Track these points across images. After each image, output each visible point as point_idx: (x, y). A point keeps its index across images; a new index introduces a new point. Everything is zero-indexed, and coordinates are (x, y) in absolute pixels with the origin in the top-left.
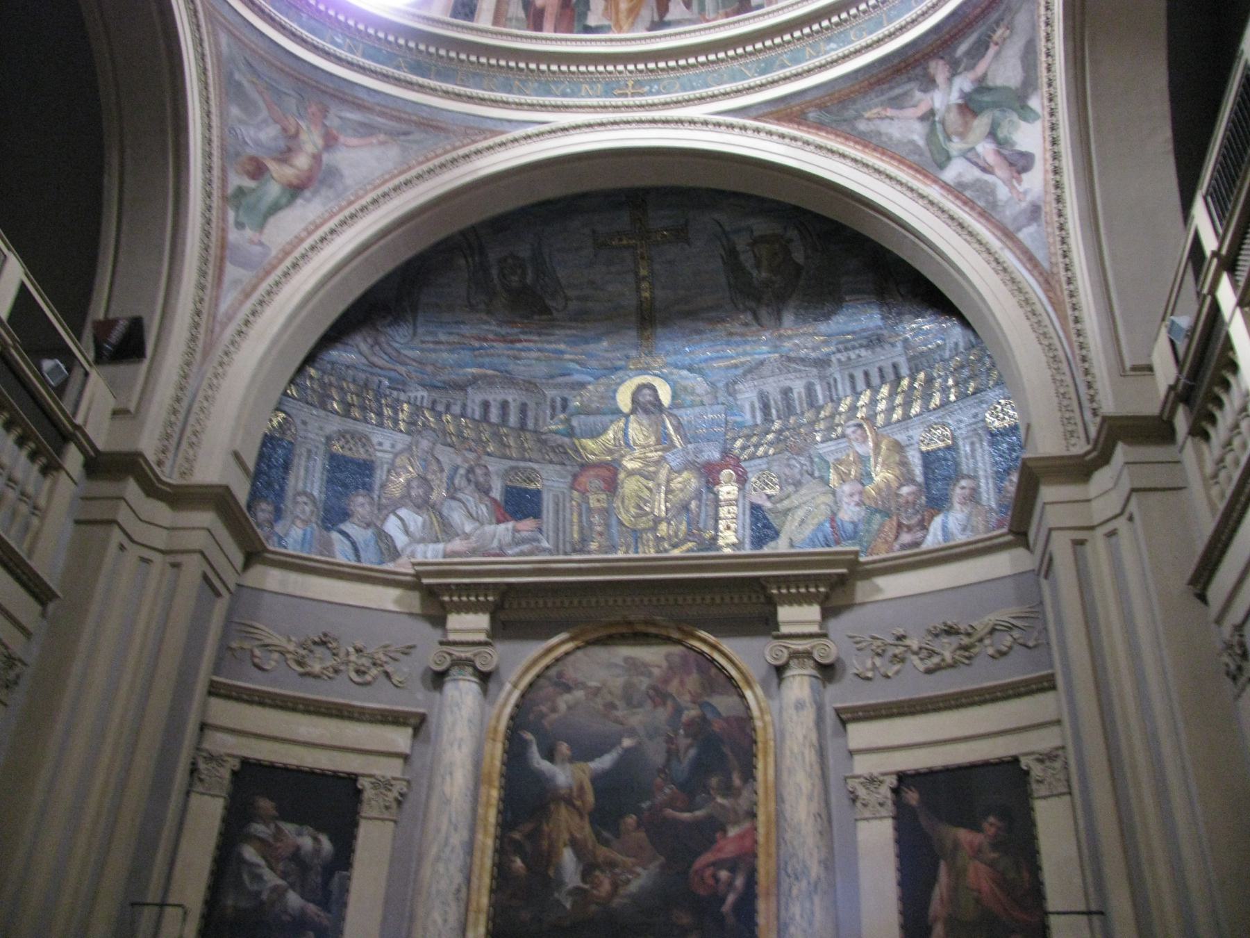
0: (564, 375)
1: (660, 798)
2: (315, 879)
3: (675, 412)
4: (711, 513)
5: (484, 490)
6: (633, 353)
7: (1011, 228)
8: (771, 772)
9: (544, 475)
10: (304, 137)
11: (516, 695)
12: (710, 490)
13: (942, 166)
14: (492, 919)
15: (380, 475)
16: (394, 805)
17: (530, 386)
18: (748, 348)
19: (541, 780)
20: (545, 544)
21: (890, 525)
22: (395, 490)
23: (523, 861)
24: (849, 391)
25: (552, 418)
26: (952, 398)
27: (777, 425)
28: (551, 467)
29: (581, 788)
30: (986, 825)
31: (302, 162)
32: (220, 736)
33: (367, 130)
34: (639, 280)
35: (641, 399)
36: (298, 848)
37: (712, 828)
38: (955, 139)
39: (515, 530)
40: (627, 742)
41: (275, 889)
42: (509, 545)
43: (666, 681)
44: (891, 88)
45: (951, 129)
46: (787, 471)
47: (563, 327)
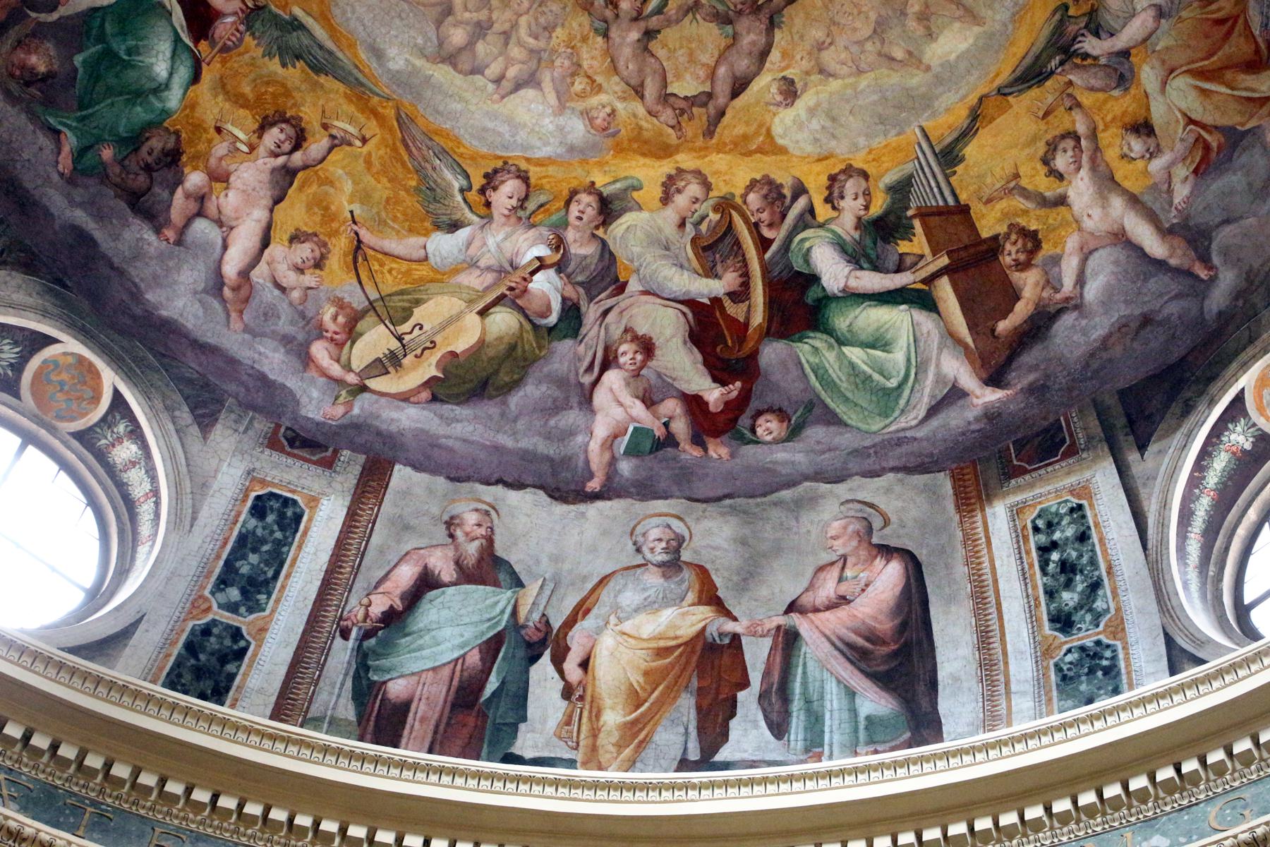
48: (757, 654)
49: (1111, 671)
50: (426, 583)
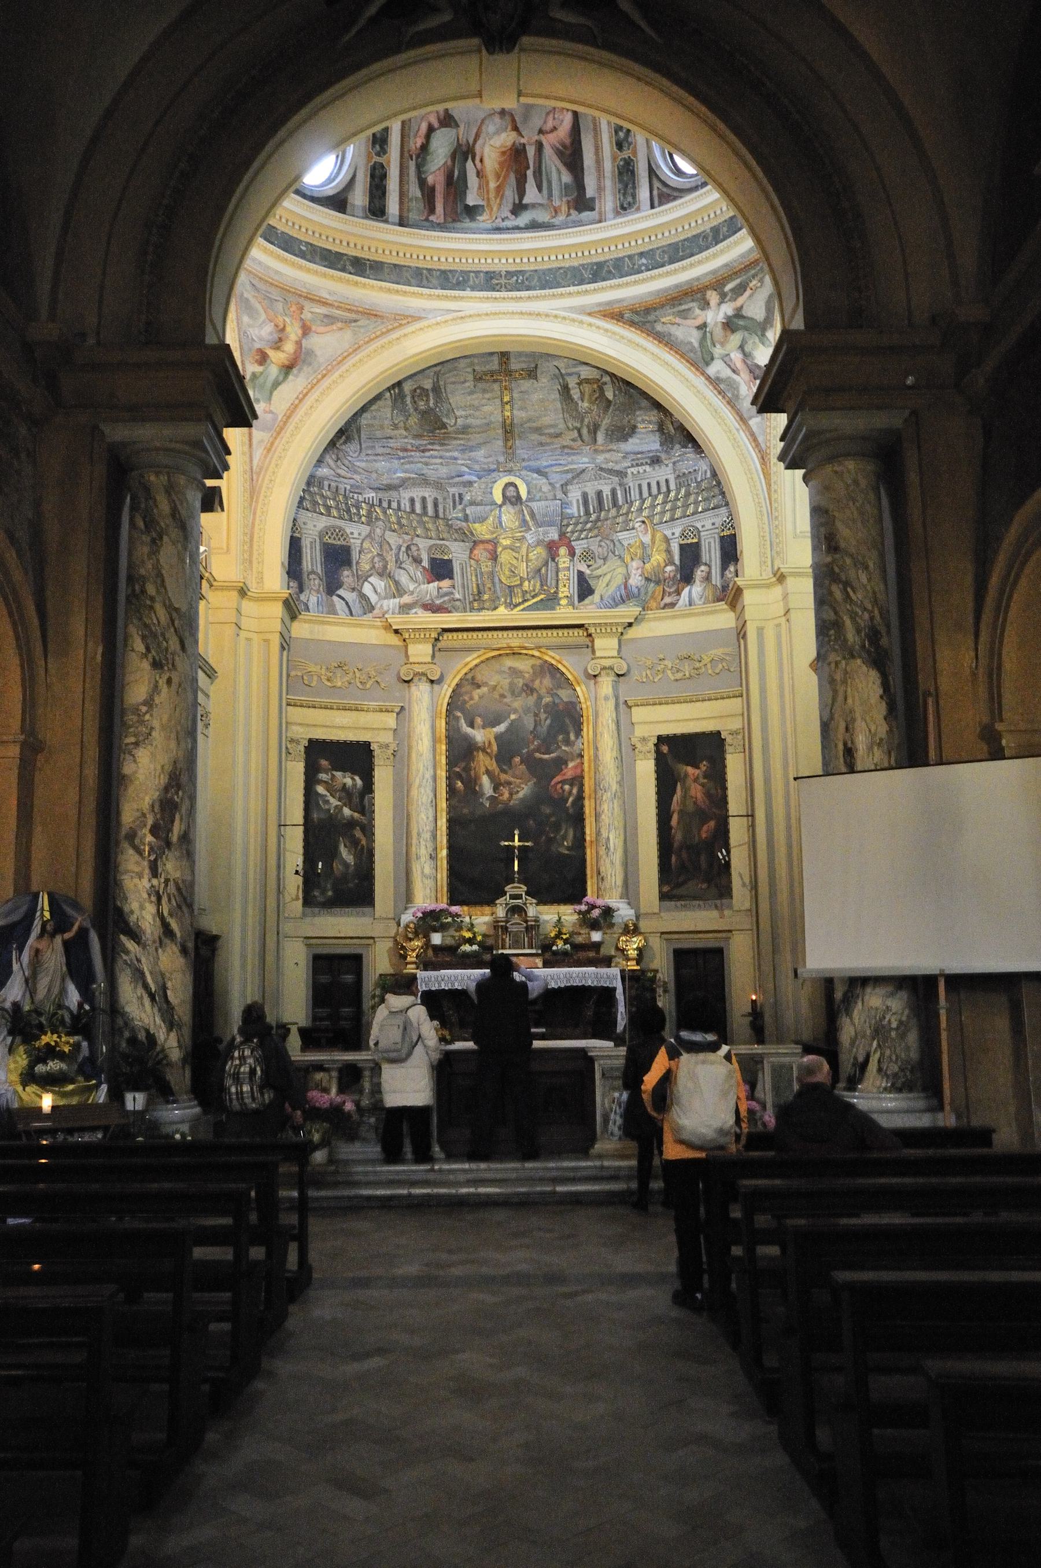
0: (459, 476)
1: (532, 747)
2: (356, 800)
3: (529, 504)
4: (554, 575)
5: (417, 561)
6: (502, 459)
7: (745, 416)
8: (591, 733)
9: (453, 550)
10: (288, 329)
11: (450, 690)
12: (553, 560)
13: (707, 364)
14: (448, 813)
15: (355, 555)
16: (392, 757)
17: (438, 485)
18: (574, 458)
19: (467, 738)
20: (457, 596)
21: (659, 589)
22: (366, 566)
23: (462, 782)
24: (638, 497)
25: (454, 508)
26: (700, 509)
27: (593, 517)
28: (456, 543)
29: (490, 742)
30: (701, 766)
31: (289, 347)
32: (294, 728)
33: (329, 320)
34: (503, 404)
35: (508, 494)
36: (345, 784)
37: (560, 763)
38: (718, 346)
39: (439, 588)
40: (513, 717)
41: (336, 806)
42: (437, 597)
43: (533, 681)
44: (680, 304)
45: (715, 338)
46: (600, 549)
47: (455, 439)
48: (531, 152)
49: (633, 172)
50: (431, 129)
